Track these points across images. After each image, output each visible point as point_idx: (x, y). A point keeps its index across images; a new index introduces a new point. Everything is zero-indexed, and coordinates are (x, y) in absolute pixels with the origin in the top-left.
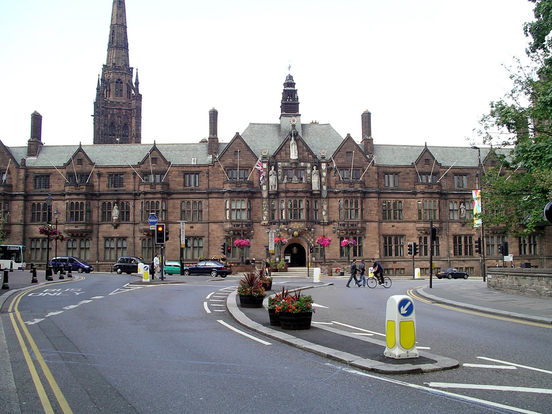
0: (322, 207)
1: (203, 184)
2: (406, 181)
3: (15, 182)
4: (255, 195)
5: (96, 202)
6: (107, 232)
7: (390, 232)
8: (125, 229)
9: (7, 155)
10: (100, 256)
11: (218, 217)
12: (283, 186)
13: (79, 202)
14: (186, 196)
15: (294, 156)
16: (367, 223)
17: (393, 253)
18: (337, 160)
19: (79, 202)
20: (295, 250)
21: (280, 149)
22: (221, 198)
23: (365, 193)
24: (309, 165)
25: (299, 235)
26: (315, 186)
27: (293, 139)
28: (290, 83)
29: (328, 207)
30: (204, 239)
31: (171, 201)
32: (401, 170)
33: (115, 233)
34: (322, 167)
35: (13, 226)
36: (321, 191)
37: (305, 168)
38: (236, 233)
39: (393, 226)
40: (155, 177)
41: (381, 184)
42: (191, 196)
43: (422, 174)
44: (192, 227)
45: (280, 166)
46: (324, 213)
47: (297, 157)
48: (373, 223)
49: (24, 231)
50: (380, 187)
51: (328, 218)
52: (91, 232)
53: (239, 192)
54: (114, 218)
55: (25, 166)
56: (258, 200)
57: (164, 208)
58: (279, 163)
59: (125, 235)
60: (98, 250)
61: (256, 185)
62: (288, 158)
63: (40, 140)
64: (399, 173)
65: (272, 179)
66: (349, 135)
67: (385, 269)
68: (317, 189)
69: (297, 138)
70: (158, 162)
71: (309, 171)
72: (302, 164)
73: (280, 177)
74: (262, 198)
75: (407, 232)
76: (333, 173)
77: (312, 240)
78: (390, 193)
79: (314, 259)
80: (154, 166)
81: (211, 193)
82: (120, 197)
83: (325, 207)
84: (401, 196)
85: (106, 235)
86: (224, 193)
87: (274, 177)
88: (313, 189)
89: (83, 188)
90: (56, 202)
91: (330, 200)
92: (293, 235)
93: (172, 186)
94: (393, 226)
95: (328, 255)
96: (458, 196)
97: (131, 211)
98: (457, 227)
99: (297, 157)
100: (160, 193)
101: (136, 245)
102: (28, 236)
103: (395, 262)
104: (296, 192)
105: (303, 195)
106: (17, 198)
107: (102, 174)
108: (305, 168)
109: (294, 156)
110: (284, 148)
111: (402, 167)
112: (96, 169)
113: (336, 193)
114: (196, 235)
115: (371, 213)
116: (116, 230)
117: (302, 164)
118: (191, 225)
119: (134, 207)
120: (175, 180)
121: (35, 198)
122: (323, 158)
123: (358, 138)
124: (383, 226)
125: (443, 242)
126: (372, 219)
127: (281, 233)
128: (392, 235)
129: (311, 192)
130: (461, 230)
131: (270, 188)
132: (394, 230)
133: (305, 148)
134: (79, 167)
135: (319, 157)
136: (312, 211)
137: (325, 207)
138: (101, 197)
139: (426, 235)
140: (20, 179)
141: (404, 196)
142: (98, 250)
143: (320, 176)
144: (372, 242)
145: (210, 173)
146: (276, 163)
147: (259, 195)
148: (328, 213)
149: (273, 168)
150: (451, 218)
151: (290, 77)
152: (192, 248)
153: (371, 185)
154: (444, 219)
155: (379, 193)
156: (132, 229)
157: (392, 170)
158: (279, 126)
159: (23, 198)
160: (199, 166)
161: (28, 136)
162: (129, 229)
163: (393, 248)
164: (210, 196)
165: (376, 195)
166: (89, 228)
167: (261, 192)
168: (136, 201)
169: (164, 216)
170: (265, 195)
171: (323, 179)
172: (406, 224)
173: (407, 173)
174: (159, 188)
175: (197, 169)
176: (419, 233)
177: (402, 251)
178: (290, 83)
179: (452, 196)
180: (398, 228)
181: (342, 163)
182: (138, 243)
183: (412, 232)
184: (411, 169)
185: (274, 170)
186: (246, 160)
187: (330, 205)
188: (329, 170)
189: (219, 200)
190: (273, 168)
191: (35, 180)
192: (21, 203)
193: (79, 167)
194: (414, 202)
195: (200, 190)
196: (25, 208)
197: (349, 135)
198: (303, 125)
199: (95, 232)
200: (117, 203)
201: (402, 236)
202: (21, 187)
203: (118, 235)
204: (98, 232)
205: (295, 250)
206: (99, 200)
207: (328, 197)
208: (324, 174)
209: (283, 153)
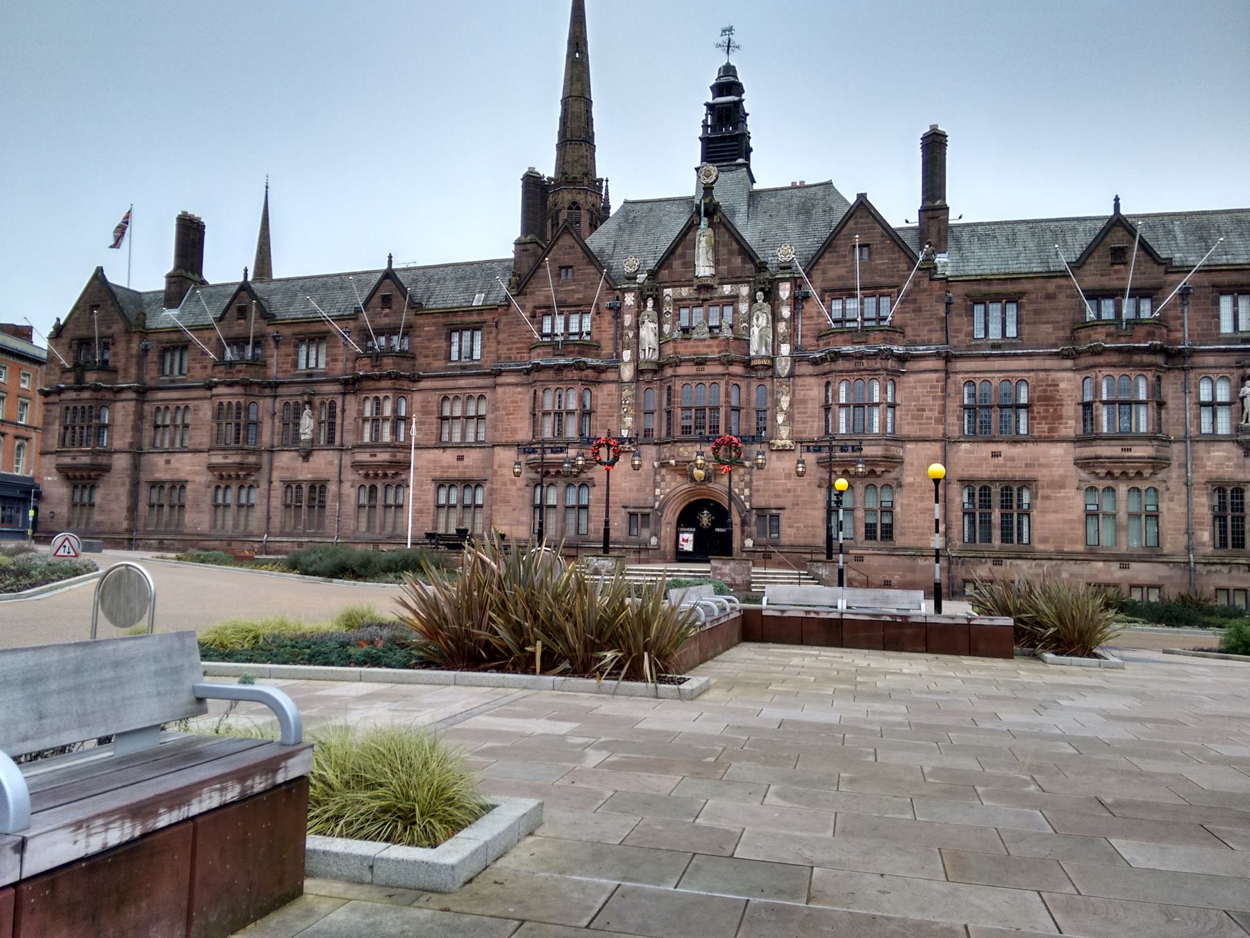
0: (777, 402)
1: (489, 352)
2: (1044, 318)
3: (123, 361)
4: (603, 376)
5: (269, 402)
6: (288, 469)
7: (985, 472)
8: (323, 464)
9: (113, 305)
10: (271, 525)
11: (514, 431)
12: (669, 350)
13: (234, 402)
14: (450, 383)
15: (704, 269)
16: (909, 446)
17: (996, 533)
18: (824, 272)
19: (234, 402)
20: (705, 518)
21: (671, 252)
22: (523, 385)
23: (902, 359)
24: (744, 290)
25: (707, 479)
26: (756, 347)
27: (704, 222)
28: (728, 85)
29: (791, 405)
30: (487, 486)
31: (418, 398)
32: (1027, 286)
33: (305, 472)
34: (781, 293)
35: (116, 456)
36: (773, 360)
37: (733, 300)
38: (553, 471)
39: (995, 455)
40: (389, 340)
41: (958, 331)
42: (462, 382)
43: (1096, 295)
44: (460, 458)
45: (668, 298)
46: (780, 419)
47: (712, 271)
48: (927, 445)
49: (136, 467)
50: (953, 341)
51: (792, 432)
52: (257, 468)
53: (560, 369)
54: (303, 437)
55: (144, 327)
56: (613, 387)
57: (403, 414)
58: (667, 291)
59: (324, 476)
60: (268, 511)
61: (607, 349)
62: (689, 276)
63: (200, 274)
64: (1022, 294)
65: (648, 333)
66: (862, 198)
67: (966, 581)
68: (763, 352)
69: (716, 219)
70: (395, 306)
71: (744, 308)
72: (727, 289)
73: (667, 328)
74: (619, 381)
75: (1044, 471)
76: (809, 308)
77: (747, 492)
78: (986, 357)
79: (749, 543)
80: (386, 315)
81: (498, 373)
82: (318, 388)
83: (785, 402)
84: (1024, 363)
85: (287, 475)
86: (528, 372)
87: (652, 325)
88: (752, 353)
89: (240, 371)
90: (196, 403)
91: (799, 381)
92: (693, 479)
93: (421, 361)
94: (995, 455)
95: (789, 534)
96: (1231, 360)
97: (338, 421)
98: (1229, 459)
99: (712, 271)
100: (389, 376)
101: (344, 498)
102: (144, 477)
103: (998, 561)
104: (701, 362)
105: (720, 369)
106: (124, 396)
107: (285, 338)
108: (733, 300)
109: (704, 269)
110: (679, 250)
111: (1031, 277)
112: (271, 330)
113: (815, 362)
114: (469, 474)
115: (921, 417)
116: (306, 465)
117: (727, 289)
118: (459, 452)
119: (343, 411)
120: (426, 348)
121: (161, 395)
122: (786, 267)
123: (900, 207)
124: (962, 454)
125: (1172, 505)
126: (924, 434)
127: (664, 471)
128: (992, 481)
129: (747, 364)
130: (1238, 466)
131: (642, 356)
132: (997, 466)
133: (735, 246)
134: (240, 325)
135: (772, 263)
136: (748, 415)
137: (785, 402)
138: (281, 391)
139: (1110, 483)
140: (132, 356)
141: (1036, 363)
142: (268, 511)
143: (775, 318)
144: (922, 499)
145: (501, 326)
146: (659, 290)
147: (611, 375)
148: (790, 418)
149: (650, 303)
150: (1206, 428)
151: (729, 70)
152: (459, 507)
153: (924, 334)
154: (1174, 432)
155: (948, 358)
156: (336, 462)
157: (996, 288)
158: (688, 200)
159: (133, 395)
160: (480, 311)
161: (168, 262)
162: (331, 463)
163: (996, 515)
164: (500, 380)
165: (939, 364)
166: (252, 459)
167: (618, 367)
168: (348, 398)
169: (402, 431)
170: (627, 373)
171: (782, 327)
172: (1043, 447)
173: (1050, 297)
174: (389, 365)
175: (475, 318)
176: (1084, 474)
177: (1025, 529)
178: (728, 85)
179: (1210, 360)
180: (1012, 459)
181: (840, 278)
182: (348, 496)
183: (1061, 471)
184: (1063, 282)
185: (654, 307)
186: (586, 287)
187: (800, 395)
188: (799, 300)
189: (519, 389)
190: (650, 303)
191: (162, 358)
192: (131, 406)
193: (240, 325)
194: (1069, 380)
195: (480, 367)
196: (140, 416)
197: (862, 198)
198: (754, 196)
199: (265, 466)
200: (310, 403)
201: (1026, 483)
202: (133, 371)
203: (310, 476)
204: (271, 470)
205: (705, 518)
206: (276, 397)
207: (791, 375)
208: (786, 312)
209: (677, 264)
